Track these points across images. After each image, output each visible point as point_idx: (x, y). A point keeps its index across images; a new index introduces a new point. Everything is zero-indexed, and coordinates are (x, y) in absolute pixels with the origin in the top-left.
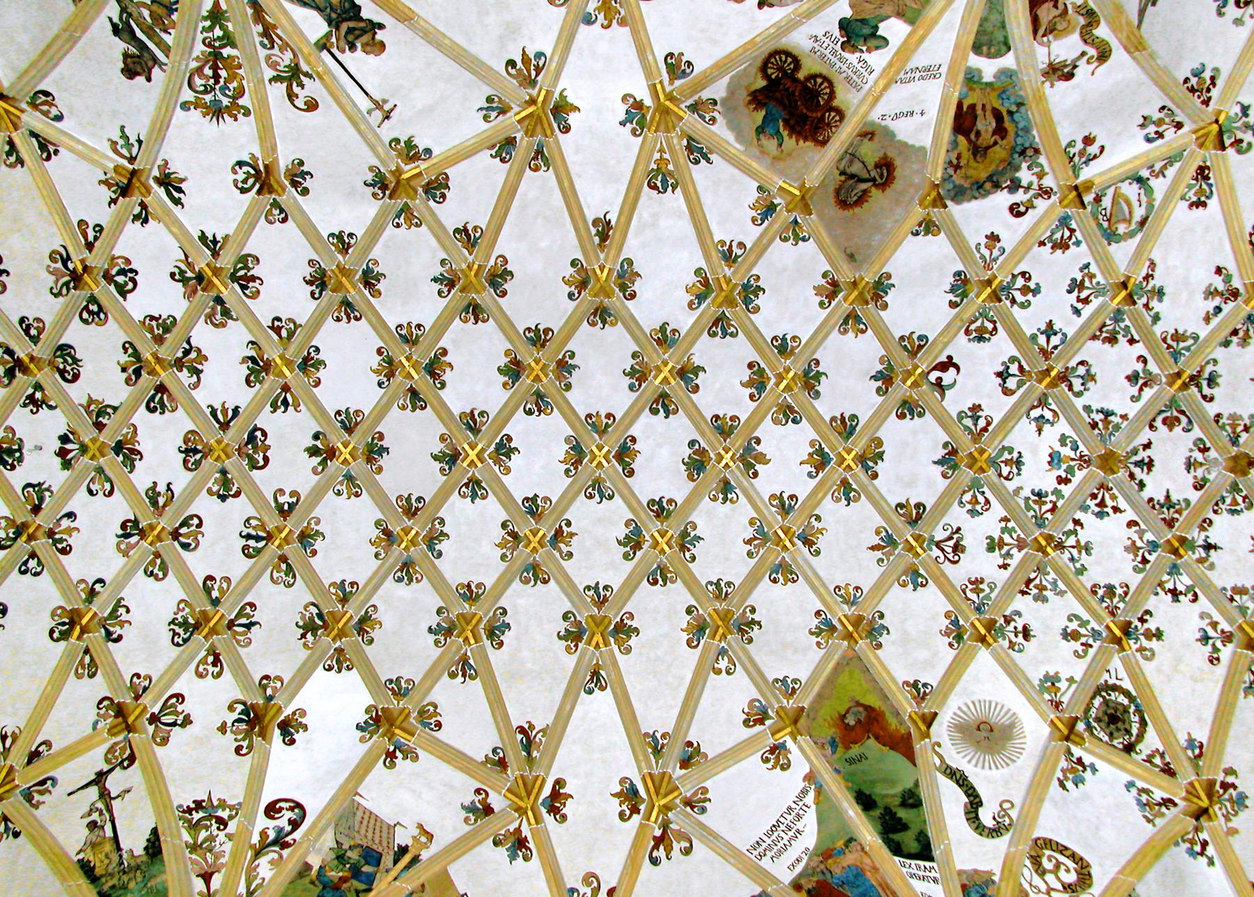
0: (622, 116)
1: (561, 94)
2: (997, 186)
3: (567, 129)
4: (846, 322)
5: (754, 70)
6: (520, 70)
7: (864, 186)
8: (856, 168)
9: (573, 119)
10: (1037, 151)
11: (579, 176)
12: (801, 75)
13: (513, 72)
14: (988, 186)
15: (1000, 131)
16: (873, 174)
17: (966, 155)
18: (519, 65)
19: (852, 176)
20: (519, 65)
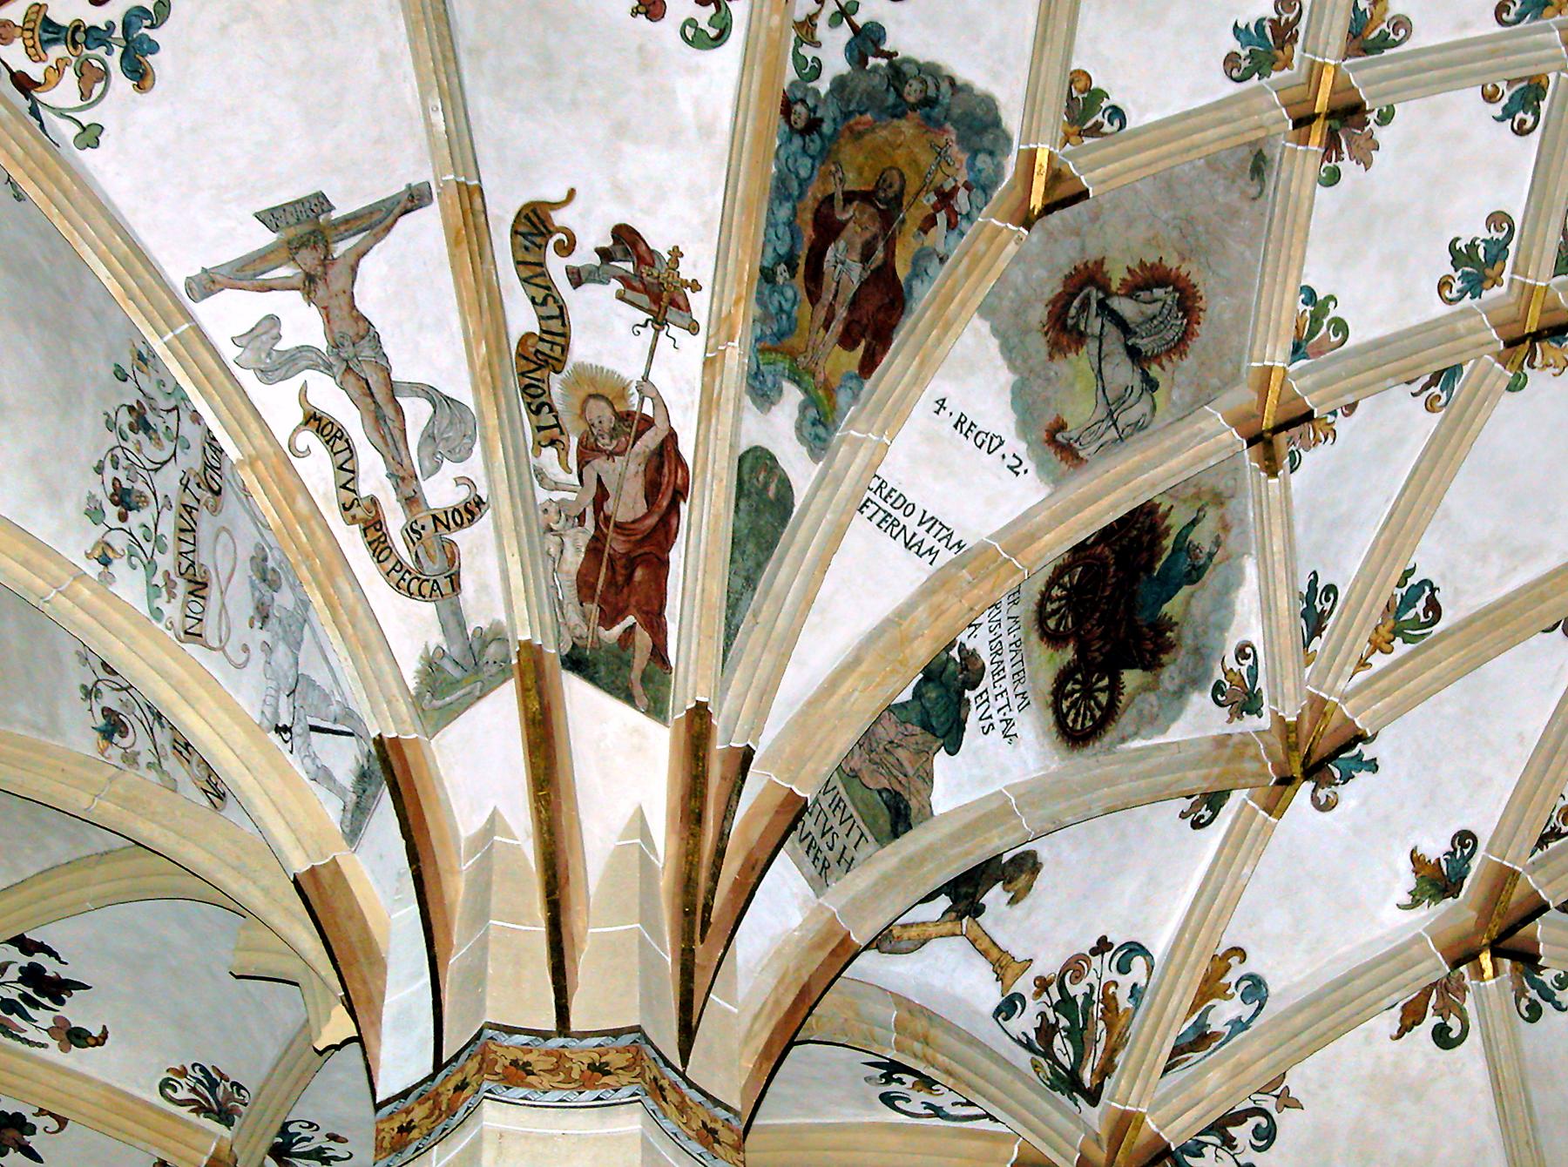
0: (1362, 778)
1: (1415, 903)
2: (898, 72)
3: (1465, 838)
4: (1383, 43)
5: (1126, 720)
6: (1437, 1012)
7: (1125, 307)
8: (1122, 373)
9: (1436, 847)
10: (787, 109)
11: (1521, 738)
12: (1069, 654)
13: (1454, 1023)
14: (912, 92)
15: (827, 228)
16: (1095, 325)
17: (912, 217)
18: (1431, 1020)
19: (1134, 353)
20: (1431, 1020)
